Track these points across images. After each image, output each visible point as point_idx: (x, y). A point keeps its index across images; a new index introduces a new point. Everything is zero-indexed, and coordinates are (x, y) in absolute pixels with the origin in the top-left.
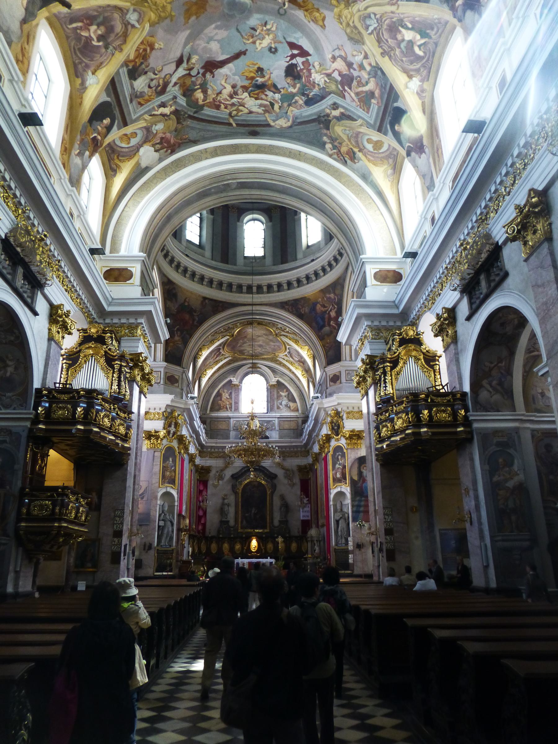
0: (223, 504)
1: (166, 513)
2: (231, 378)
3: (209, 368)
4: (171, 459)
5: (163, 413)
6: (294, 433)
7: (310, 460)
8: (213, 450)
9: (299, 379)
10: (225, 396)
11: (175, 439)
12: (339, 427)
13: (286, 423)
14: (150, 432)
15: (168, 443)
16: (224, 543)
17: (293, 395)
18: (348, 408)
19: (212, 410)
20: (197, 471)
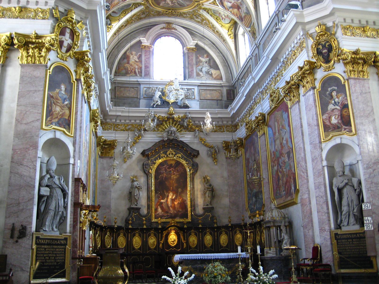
0: (132, 187)
1: (53, 174)
2: (141, 39)
3: (115, 20)
4: (63, 87)
5: (51, 10)
6: (217, 105)
7: (242, 132)
8: (118, 121)
9: (224, 40)
10: (133, 58)
11: (70, 56)
12: (330, 49)
13: (208, 92)
14: (28, 36)
15: (59, 60)
16: (134, 235)
17: (215, 62)
18: (345, 19)
19: (117, 74)
20: (98, 144)
